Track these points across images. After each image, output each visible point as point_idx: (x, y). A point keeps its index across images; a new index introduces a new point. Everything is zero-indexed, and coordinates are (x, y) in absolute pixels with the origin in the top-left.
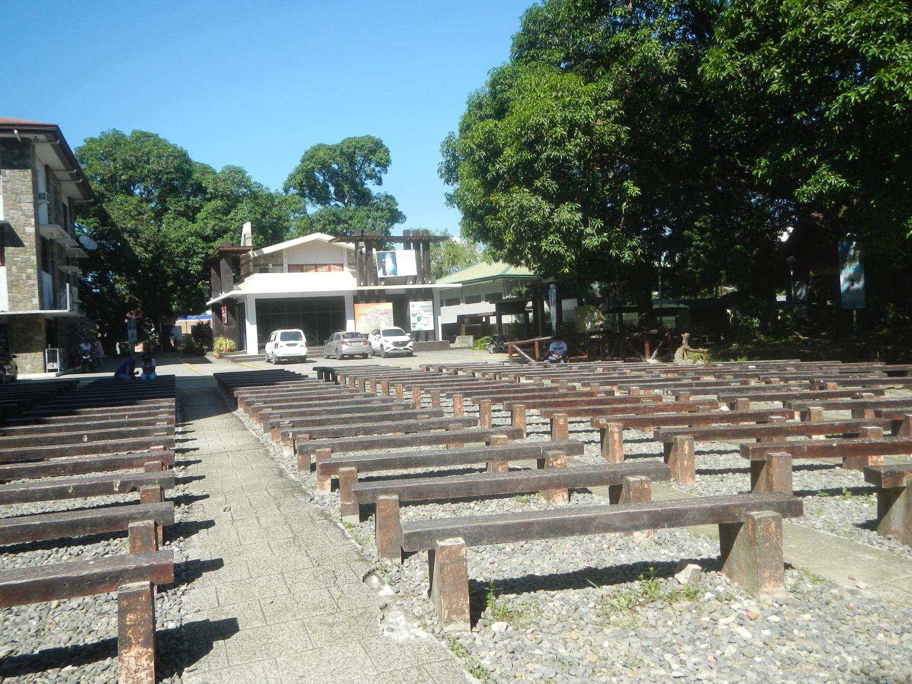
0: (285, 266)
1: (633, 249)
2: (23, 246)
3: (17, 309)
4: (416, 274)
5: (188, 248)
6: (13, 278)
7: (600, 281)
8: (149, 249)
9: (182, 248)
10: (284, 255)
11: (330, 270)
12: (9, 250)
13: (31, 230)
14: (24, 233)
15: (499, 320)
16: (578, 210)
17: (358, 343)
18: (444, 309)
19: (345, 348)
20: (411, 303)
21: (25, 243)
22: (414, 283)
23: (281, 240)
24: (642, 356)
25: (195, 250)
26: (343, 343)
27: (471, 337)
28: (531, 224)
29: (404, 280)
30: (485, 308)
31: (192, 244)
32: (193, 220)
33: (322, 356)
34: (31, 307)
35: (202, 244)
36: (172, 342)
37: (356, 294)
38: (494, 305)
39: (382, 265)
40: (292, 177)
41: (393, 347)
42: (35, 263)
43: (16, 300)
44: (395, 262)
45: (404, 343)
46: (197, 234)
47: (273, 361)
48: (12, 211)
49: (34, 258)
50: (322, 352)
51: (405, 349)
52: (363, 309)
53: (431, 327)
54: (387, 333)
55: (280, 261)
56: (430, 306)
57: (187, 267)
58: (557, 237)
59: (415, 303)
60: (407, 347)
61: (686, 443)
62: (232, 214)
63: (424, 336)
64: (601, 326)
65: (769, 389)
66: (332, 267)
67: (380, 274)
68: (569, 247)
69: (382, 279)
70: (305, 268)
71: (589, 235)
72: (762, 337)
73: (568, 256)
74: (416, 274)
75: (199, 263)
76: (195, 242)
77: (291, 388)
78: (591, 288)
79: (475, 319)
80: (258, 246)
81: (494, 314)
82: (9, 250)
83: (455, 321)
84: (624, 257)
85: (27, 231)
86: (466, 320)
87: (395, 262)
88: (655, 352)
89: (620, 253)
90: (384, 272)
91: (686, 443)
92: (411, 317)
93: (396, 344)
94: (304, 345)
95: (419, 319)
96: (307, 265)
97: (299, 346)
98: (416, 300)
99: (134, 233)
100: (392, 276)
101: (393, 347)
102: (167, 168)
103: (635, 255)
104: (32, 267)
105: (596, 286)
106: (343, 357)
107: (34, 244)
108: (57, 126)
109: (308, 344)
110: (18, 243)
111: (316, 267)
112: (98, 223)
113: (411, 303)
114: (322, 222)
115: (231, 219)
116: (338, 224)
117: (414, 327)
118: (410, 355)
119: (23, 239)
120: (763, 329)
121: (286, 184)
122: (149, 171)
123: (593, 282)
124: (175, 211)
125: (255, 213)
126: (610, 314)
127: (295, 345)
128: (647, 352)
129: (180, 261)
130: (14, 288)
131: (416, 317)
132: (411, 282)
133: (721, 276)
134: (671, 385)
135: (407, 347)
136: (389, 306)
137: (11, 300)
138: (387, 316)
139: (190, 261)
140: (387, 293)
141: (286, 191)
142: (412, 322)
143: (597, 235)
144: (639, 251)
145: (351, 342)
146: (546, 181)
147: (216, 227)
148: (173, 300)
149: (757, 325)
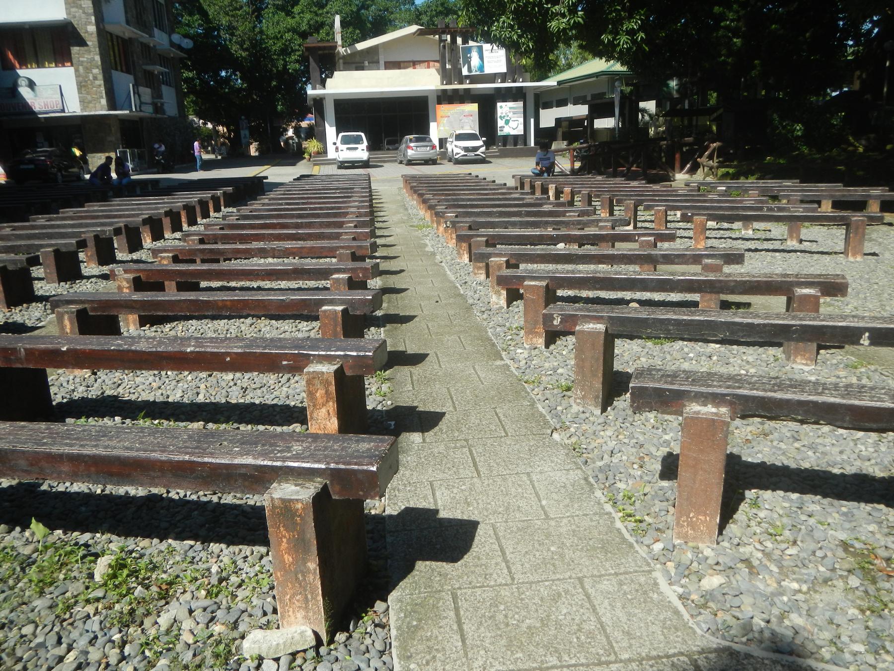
0: (382, 63)
1: (632, 33)
2: (86, 45)
3: (87, 110)
4: (505, 71)
5: (285, 44)
6: (81, 79)
7: (680, 78)
8: (245, 46)
9: (279, 45)
10: (381, 51)
11: (429, 67)
12: (75, 50)
13: (92, 28)
14: (87, 32)
15: (592, 124)
17: (425, 148)
18: (543, 113)
19: (410, 152)
20: (499, 104)
21: (89, 43)
22: (503, 81)
23: (382, 32)
24: (670, 170)
26: (409, 147)
27: (565, 143)
29: (492, 78)
30: (581, 110)
31: (289, 40)
32: (289, 13)
33: (396, 161)
34: (100, 108)
35: (299, 41)
36: (282, 143)
37: (440, 94)
39: (468, 61)
41: (463, 153)
42: (100, 63)
43: (86, 101)
44: (481, 58)
45: (476, 149)
46: (294, 30)
47: (405, 162)
48: (73, 10)
49: (98, 58)
50: (396, 157)
51: (476, 155)
52: (444, 110)
53: (520, 131)
54: (460, 137)
55: (376, 58)
57: (285, 66)
59: (503, 104)
61: (66, 317)
62: (329, 6)
64: (663, 132)
65: (573, 224)
66: (432, 64)
67: (465, 72)
68: (524, 32)
69: (467, 77)
70: (402, 65)
71: (557, 14)
72: (805, 150)
73: (524, 44)
74: (505, 71)
75: (297, 61)
76: (292, 38)
77: (166, 201)
78: (667, 86)
79: (573, 122)
80: (350, 41)
82: (75, 50)
84: (619, 44)
85: (89, 30)
86: (564, 124)
87: (481, 58)
88: (688, 166)
89: (614, 39)
90: (470, 70)
91: (66, 317)
92: (499, 120)
93: (466, 149)
94: (365, 149)
95: (507, 122)
96: (404, 62)
97: (359, 150)
100: (478, 73)
101: (463, 153)
103: (634, 42)
104: (97, 67)
105: (673, 83)
106: (410, 163)
107: (96, 43)
110: (82, 43)
111: (414, 64)
112: (202, 21)
113: (499, 104)
114: (429, 14)
115: (327, 13)
116: (447, 15)
117: (501, 131)
118: (483, 161)
119: (86, 39)
120: (807, 138)
123: (671, 79)
124: (274, 5)
125: (350, 5)
126: (668, 118)
127: (357, 148)
128: (677, 165)
130: (83, 89)
131: (504, 120)
132: (499, 81)
134: (497, 212)
136: (474, 108)
137: (82, 101)
138: (471, 118)
139: (287, 59)
140: (472, 93)
142: (499, 125)
143: (570, 14)
144: (642, 35)
145: (417, 147)
147: (312, 22)
148: (278, 101)
149: (799, 133)
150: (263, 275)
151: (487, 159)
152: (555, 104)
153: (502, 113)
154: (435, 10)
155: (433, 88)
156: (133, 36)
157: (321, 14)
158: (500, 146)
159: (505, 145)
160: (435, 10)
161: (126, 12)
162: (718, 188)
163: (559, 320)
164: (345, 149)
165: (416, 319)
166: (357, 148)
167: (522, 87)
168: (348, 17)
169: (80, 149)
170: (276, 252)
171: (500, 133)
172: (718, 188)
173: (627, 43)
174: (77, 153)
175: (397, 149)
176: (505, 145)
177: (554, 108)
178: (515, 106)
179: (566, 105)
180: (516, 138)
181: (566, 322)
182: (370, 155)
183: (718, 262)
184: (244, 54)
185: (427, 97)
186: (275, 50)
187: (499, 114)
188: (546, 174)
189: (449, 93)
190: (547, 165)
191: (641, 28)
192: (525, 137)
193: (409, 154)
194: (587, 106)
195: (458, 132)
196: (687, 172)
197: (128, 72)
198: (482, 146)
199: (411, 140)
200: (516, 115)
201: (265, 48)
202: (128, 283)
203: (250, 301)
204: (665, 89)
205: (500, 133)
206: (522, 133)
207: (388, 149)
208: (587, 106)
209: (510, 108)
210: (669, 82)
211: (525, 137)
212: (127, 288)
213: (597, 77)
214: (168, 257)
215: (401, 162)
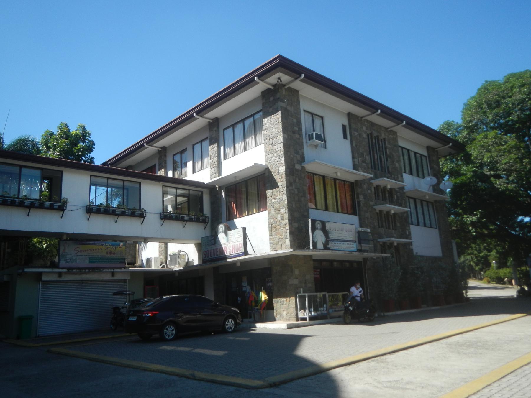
6: (272, 220)
13: (282, 169)
49: (285, 197)
99: (493, 165)
108: (280, 57)
110: (274, 185)
130: (273, 230)
137: (272, 243)
156: (359, 178)
161: (353, 158)
169: (268, 294)
174: (263, 296)
184: (511, 186)
197: (354, 213)
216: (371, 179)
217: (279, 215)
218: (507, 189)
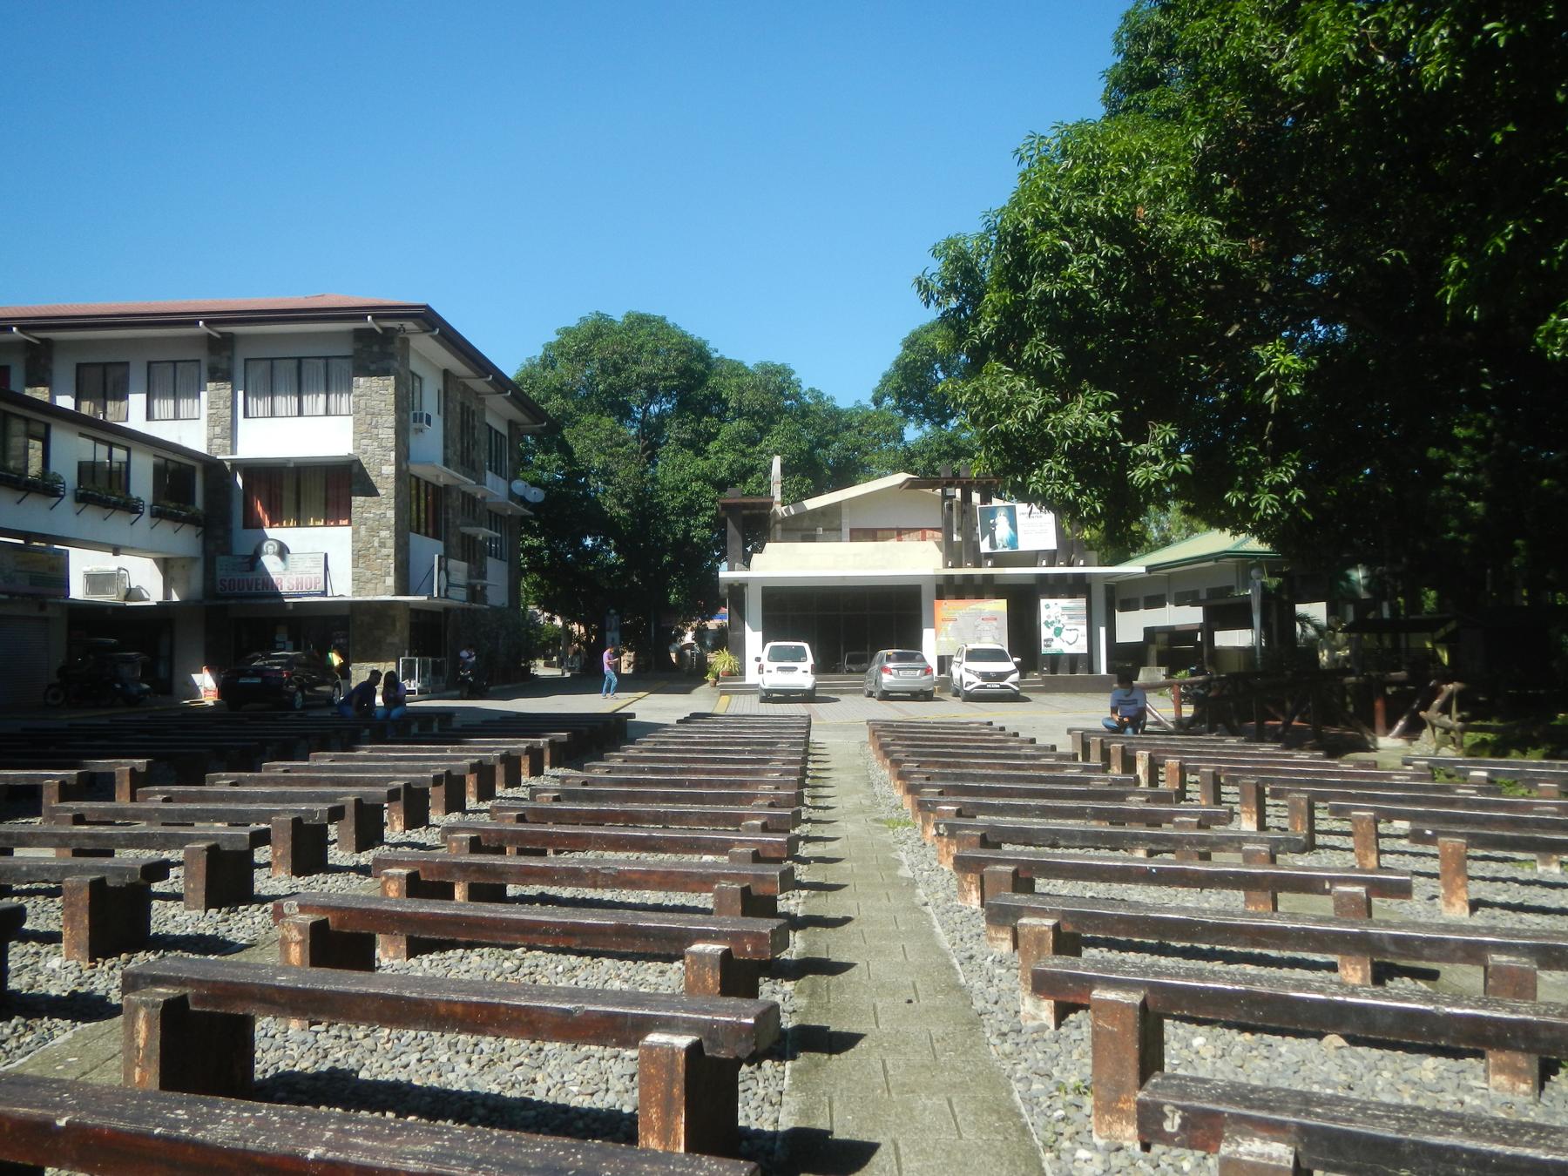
0: (846, 531)
1: (1280, 489)
2: (378, 495)
3: (363, 592)
4: (1054, 547)
5: (690, 499)
6: (360, 545)
7: (1368, 563)
8: (626, 501)
10: (845, 511)
11: (924, 539)
12: (357, 501)
13: (389, 470)
14: (380, 474)
16: (1109, 407)
18: (1121, 618)
19: (887, 679)
20: (1043, 602)
21: (380, 491)
22: (1051, 564)
23: (851, 483)
24: (1365, 729)
25: (700, 505)
26: (885, 670)
27: (1163, 670)
28: (1005, 436)
29: (1032, 558)
30: (1190, 616)
32: (700, 453)
33: (861, 692)
34: (383, 591)
35: (713, 494)
36: (673, 655)
38: (1200, 610)
39: (990, 531)
40: (887, 378)
41: (979, 682)
42: (393, 522)
43: (363, 579)
44: (1013, 525)
45: (1001, 676)
46: (705, 478)
47: (877, 694)
48: (365, 442)
49: (391, 514)
50: (861, 685)
51: (1002, 687)
53: (1081, 647)
54: (974, 655)
56: (1080, 608)
57: (686, 532)
58: (1059, 463)
60: (1005, 683)
61: (142, 1014)
62: (764, 443)
63: (1067, 664)
64: (1347, 659)
65: (1190, 843)
66: (929, 533)
67: (985, 547)
68: (1086, 486)
69: (988, 556)
70: (879, 534)
71: (1144, 458)
74: (1054, 547)
75: (707, 525)
76: (701, 491)
77: (449, 753)
78: (1347, 579)
79: (1176, 635)
80: (795, 495)
81: (1201, 628)
82: (357, 501)
83: (1139, 638)
84: (1257, 508)
85: (384, 472)
86: (1161, 638)
87: (1013, 525)
88: (1401, 723)
89: (1249, 499)
90: (993, 544)
92: (1043, 628)
93: (986, 676)
94: (809, 670)
95: (1058, 632)
97: (799, 673)
98: (1053, 595)
100: (1007, 550)
101: (979, 682)
102: (666, 369)
103: (1285, 504)
104: (388, 528)
105: (1358, 575)
106: (886, 696)
107: (392, 492)
108: (427, 307)
109: (818, 669)
110: (370, 490)
111: (899, 533)
112: (564, 461)
113: (1043, 602)
114: (926, 456)
115: (761, 452)
116: (956, 458)
118: (1014, 697)
119: (377, 485)
121: (877, 391)
122: (638, 376)
123: (1353, 566)
124: (678, 439)
125: (799, 441)
126: (1354, 635)
127: (795, 669)
128: (1380, 720)
129: (677, 522)
130: (361, 561)
131: (1053, 628)
132: (1044, 563)
133: (1515, 552)
135: (1005, 683)
136: (1000, 606)
137: (356, 579)
138: (995, 623)
140: (998, 582)
141: (877, 401)
143: (1167, 458)
144: (1297, 494)
145: (899, 669)
146: (1041, 349)
147: (735, 466)
148: (672, 586)
150: (557, 934)
151: (1022, 694)
152: (1142, 602)
153: (1049, 617)
154: (937, 451)
155: (931, 572)
156: (450, 482)
157: (751, 454)
158: (1044, 672)
159: (1054, 670)
160: (937, 451)
161: (446, 447)
162: (1473, 773)
163: (1178, 1121)
164: (774, 670)
165: (862, 1044)
166: (795, 669)
167: (1083, 575)
168: (794, 458)
169: (341, 655)
170: (599, 878)
171: (1044, 650)
172: (1473, 773)
173: (1272, 506)
174: (336, 660)
175: (864, 671)
176: (1054, 670)
177: (1142, 611)
178: (1071, 605)
179: (1162, 605)
180: (1073, 660)
181: (1195, 1127)
182: (817, 679)
183: (1524, 962)
184: (623, 512)
185: (919, 587)
186: (674, 508)
187: (1043, 618)
188: (1129, 730)
189: (957, 582)
190: (1132, 714)
191: (1296, 482)
192: (1089, 659)
193: (884, 681)
194: (1201, 608)
195: (971, 646)
196: (1401, 735)
197: (436, 536)
198: (1013, 672)
199: (889, 658)
200: (1073, 621)
201: (658, 504)
202: (300, 932)
203: (503, 1009)
204: (1344, 584)
205: (1044, 650)
206: (1085, 651)
207: (850, 671)
208: (1201, 608)
209: (1064, 609)
210: (1349, 572)
211: (1089, 659)
212: (297, 943)
213: (1216, 560)
214: (400, 876)
215: (870, 695)
216: (531, 517)
217: (376, 540)
218: (619, 516)
